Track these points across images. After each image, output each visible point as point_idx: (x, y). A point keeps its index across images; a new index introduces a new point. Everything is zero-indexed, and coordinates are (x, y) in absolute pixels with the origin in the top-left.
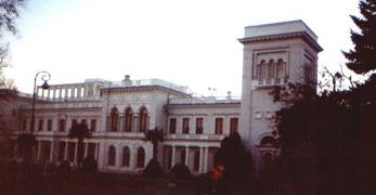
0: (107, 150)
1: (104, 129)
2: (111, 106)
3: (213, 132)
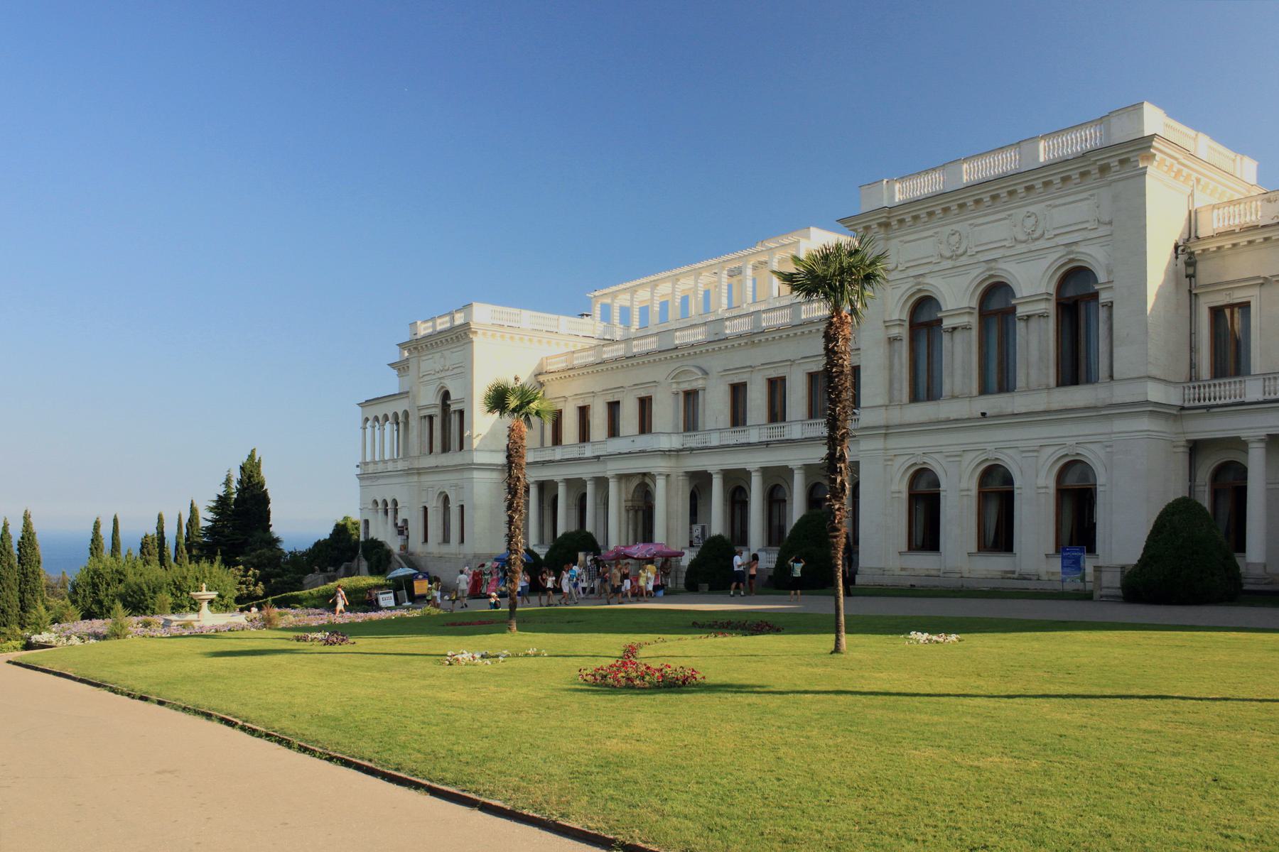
0: (901, 487)
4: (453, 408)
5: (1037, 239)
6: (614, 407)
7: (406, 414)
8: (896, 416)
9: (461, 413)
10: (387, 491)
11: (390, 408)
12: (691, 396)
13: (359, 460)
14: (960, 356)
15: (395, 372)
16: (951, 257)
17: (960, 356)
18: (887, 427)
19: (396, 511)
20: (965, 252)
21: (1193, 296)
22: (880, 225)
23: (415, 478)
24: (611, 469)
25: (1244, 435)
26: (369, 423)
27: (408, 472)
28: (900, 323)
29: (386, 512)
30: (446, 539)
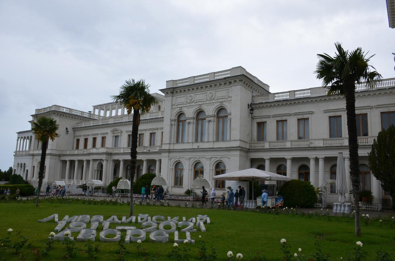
1: (166, 140)
2: (177, 110)
3: (327, 135)
5: (212, 100)
6: (95, 139)
7: (31, 137)
8: (172, 147)
10: (22, 160)
11: (26, 135)
12: (117, 137)
13: (15, 150)
14: (190, 130)
15: (30, 124)
16: (189, 103)
17: (190, 130)
18: (169, 150)
19: (25, 167)
20: (193, 102)
21: (253, 118)
22: (171, 92)
23: (32, 157)
24: (91, 158)
25: (264, 157)
26: (19, 139)
27: (30, 155)
28: (175, 121)
29: (21, 167)
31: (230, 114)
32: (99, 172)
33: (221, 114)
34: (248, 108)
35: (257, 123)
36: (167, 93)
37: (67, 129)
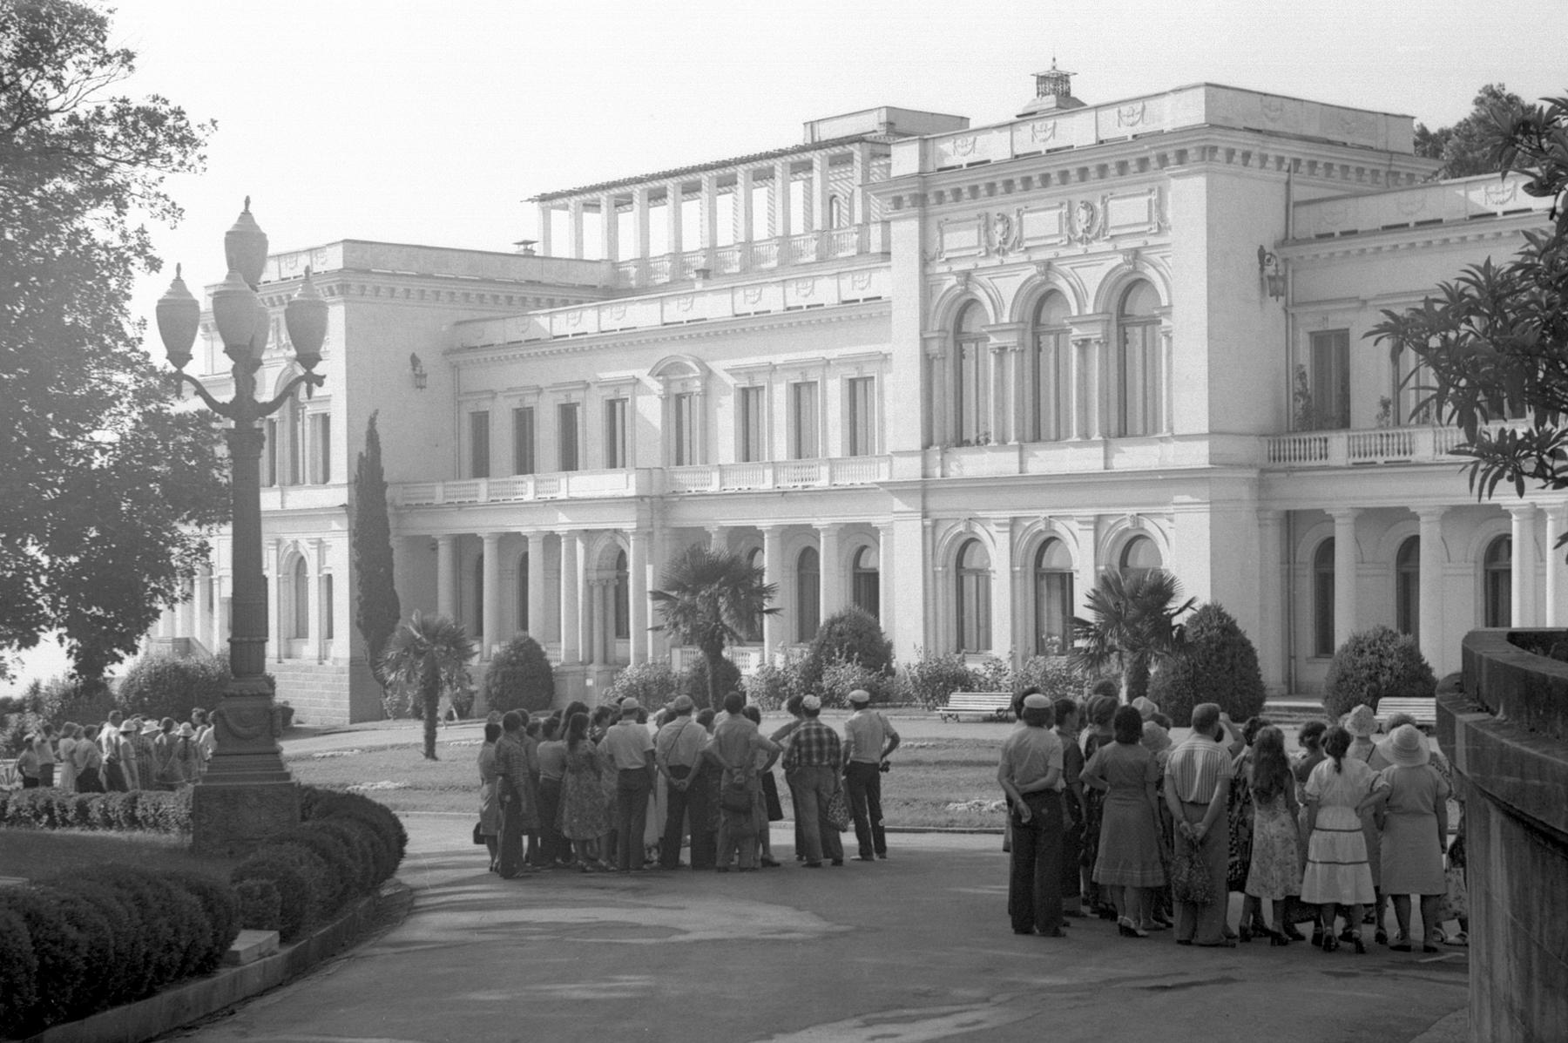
4: (310, 410)
5: (1096, 237)
6: (568, 414)
9: (326, 419)
24: (562, 523)
30: (301, 632)
31: (1167, 311)
32: (611, 592)
33: (1130, 306)
34: (1262, 269)
35: (1311, 334)
36: (898, 203)
37: (415, 360)
